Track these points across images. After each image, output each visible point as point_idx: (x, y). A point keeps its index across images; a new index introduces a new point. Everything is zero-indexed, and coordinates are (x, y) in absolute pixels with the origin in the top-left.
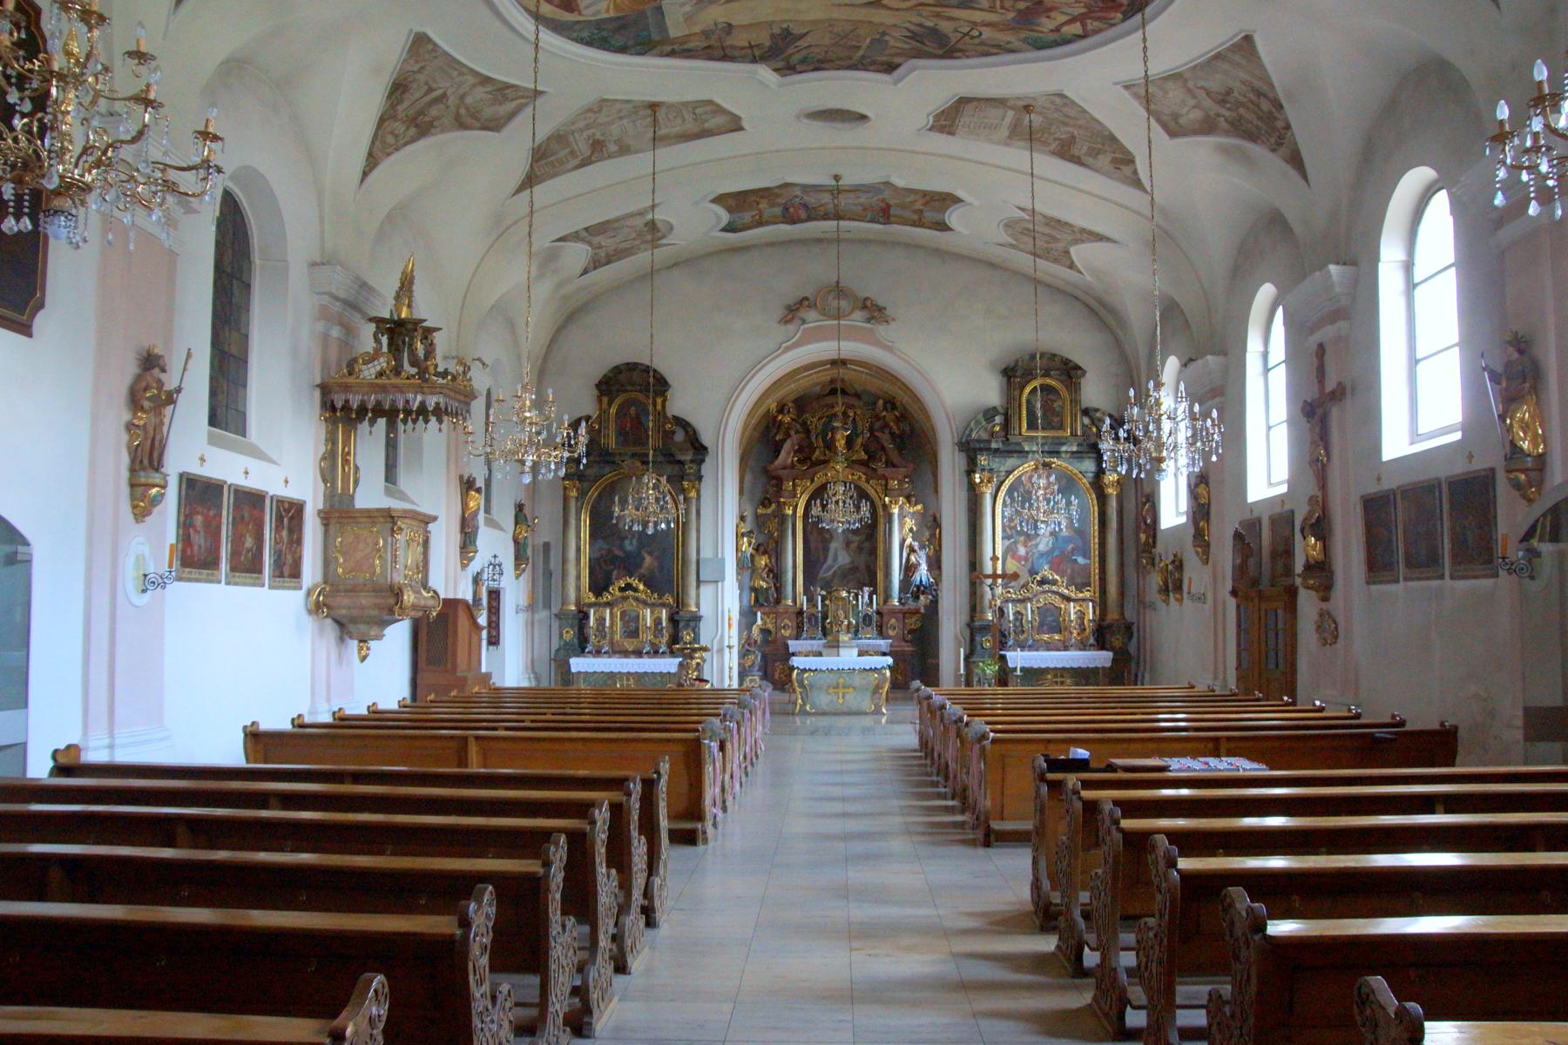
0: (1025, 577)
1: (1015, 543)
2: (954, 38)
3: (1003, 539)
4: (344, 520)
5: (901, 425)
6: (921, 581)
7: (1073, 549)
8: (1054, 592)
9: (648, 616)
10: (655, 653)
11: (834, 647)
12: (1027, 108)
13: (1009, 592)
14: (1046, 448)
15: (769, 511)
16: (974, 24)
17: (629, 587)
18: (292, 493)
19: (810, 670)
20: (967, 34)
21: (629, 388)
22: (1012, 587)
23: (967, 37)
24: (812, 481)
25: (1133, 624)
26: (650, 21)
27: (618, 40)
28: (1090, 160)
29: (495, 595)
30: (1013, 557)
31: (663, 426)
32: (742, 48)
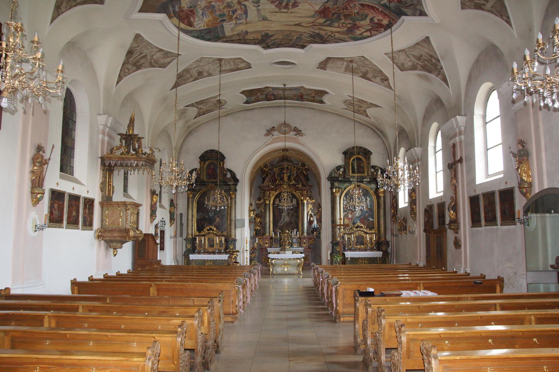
0: (351, 225)
1: (348, 213)
2: (326, 36)
3: (343, 212)
4: (108, 206)
8: (361, 231)
9: (217, 240)
10: (220, 253)
11: (267, 274)
12: (351, 61)
13: (346, 231)
14: (358, 180)
15: (261, 202)
16: (332, 32)
17: (210, 229)
18: (90, 196)
19: (275, 259)
20: (330, 35)
21: (211, 159)
22: (347, 229)
23: (330, 36)
25: (389, 242)
26: (219, 30)
27: (208, 37)
28: (373, 79)
29: (163, 232)
30: (347, 218)
31: (223, 172)
32: (251, 40)
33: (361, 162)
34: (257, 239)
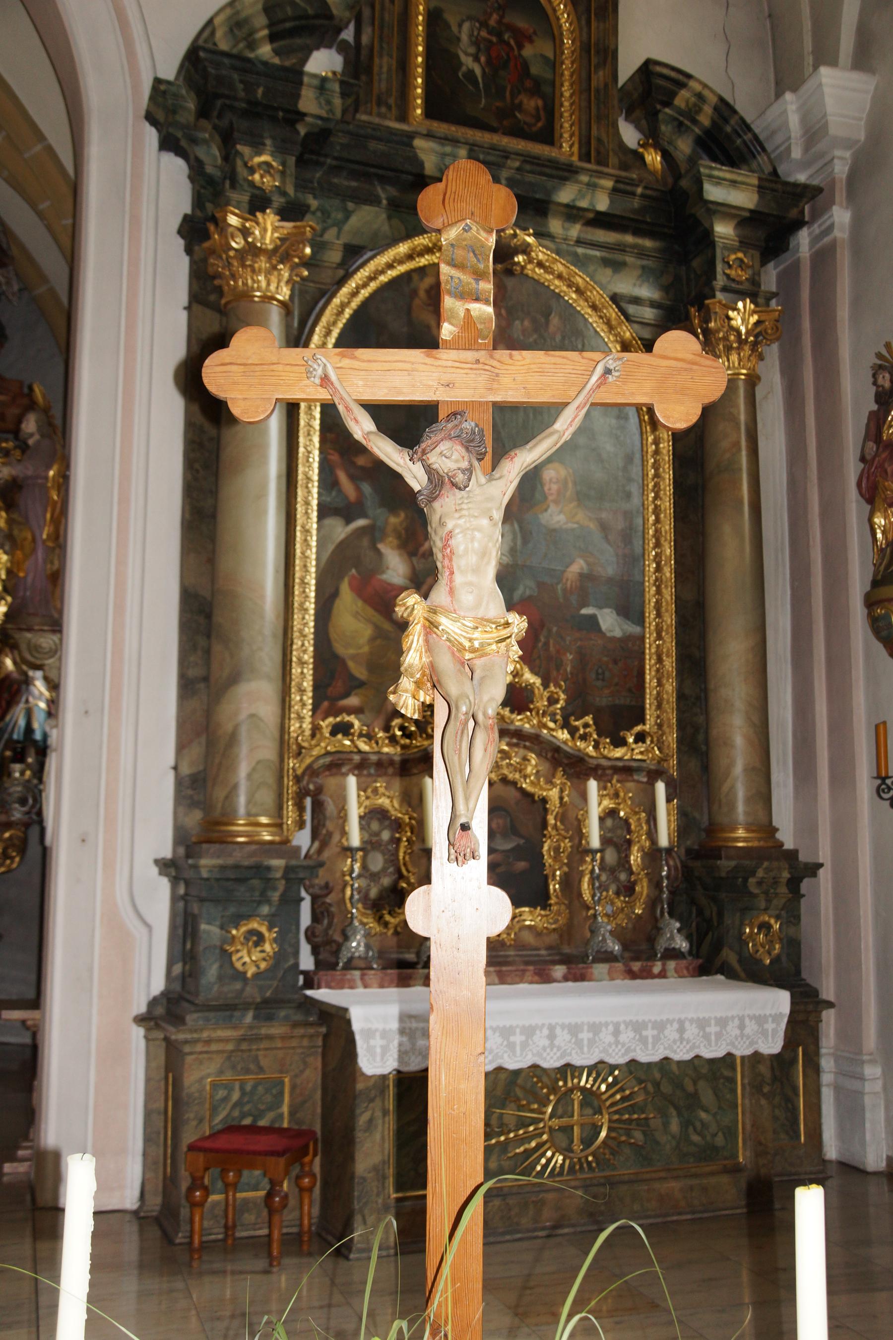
1: (373, 533)
3: (324, 512)
7: (586, 578)
30: (359, 590)
33: (522, 23)
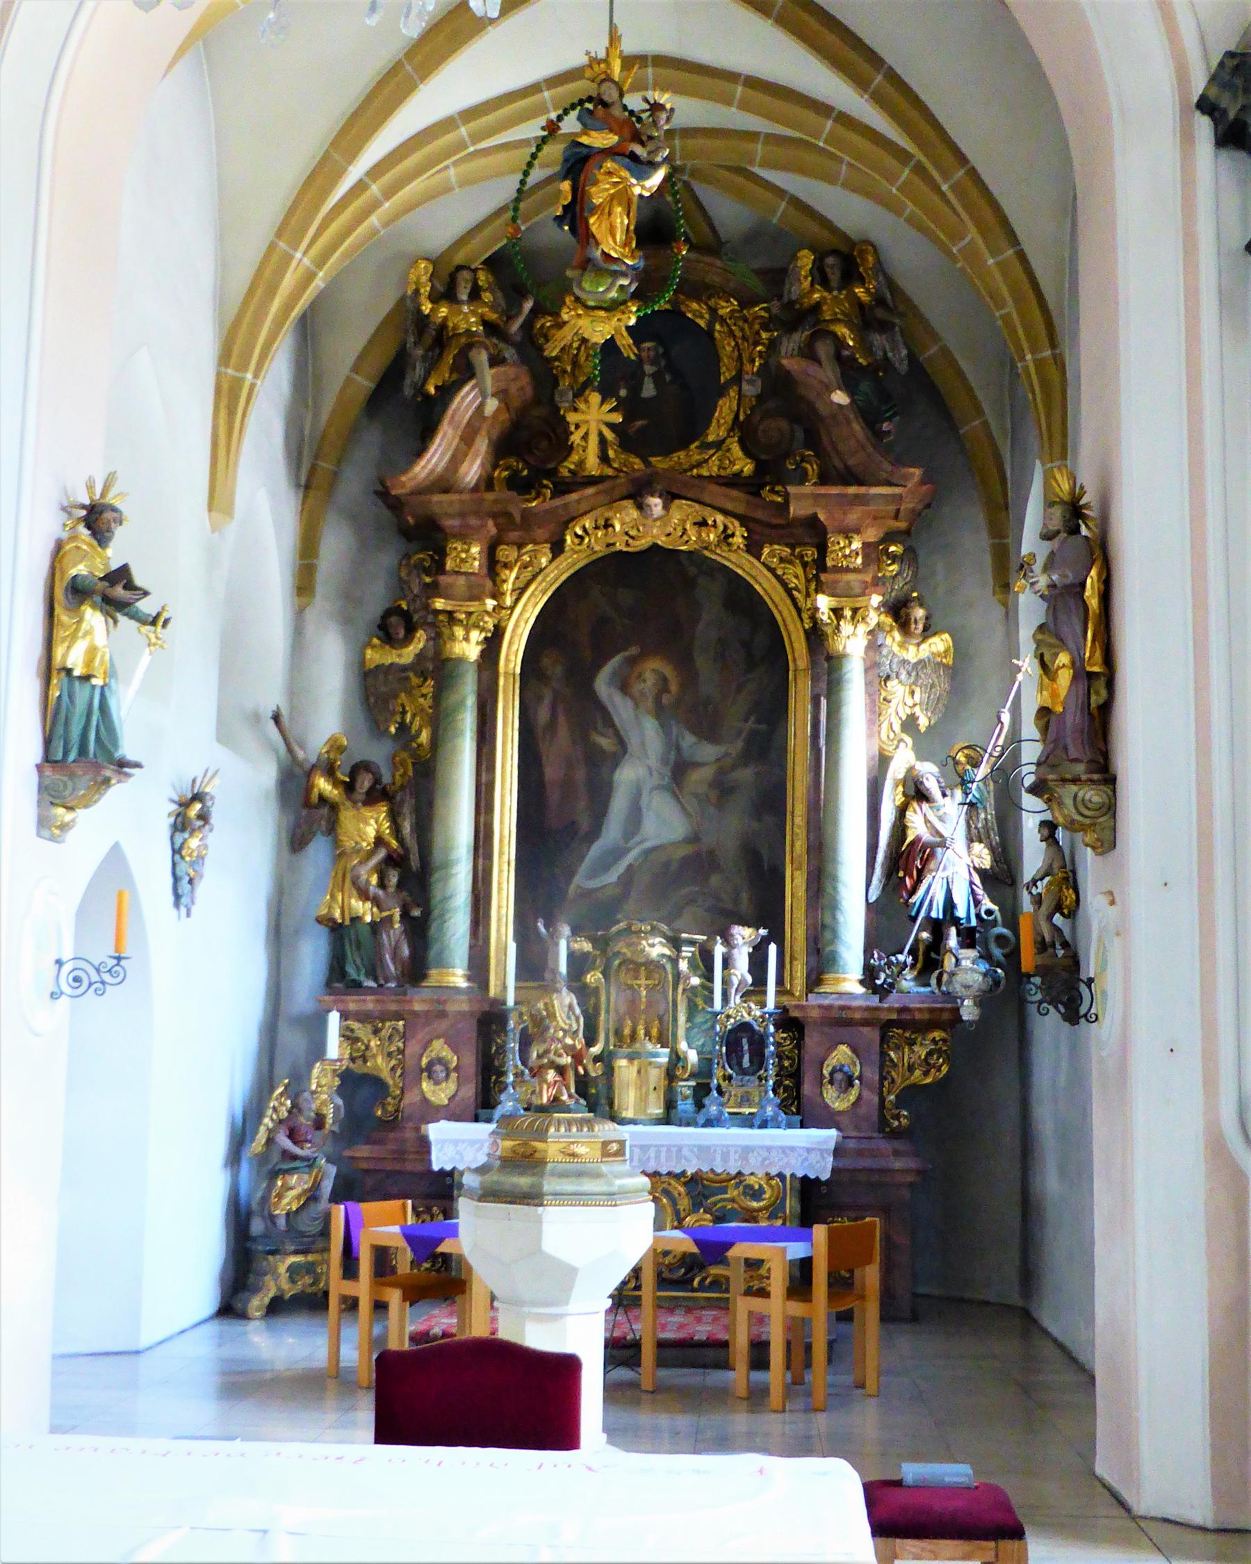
5: (878, 340)
6: (950, 905)
15: (408, 654)
24: (557, 549)
34: (334, 1018)
